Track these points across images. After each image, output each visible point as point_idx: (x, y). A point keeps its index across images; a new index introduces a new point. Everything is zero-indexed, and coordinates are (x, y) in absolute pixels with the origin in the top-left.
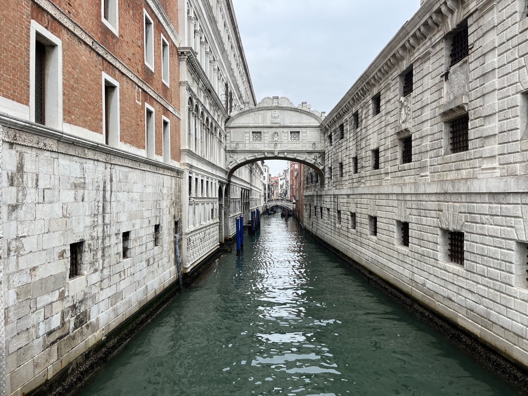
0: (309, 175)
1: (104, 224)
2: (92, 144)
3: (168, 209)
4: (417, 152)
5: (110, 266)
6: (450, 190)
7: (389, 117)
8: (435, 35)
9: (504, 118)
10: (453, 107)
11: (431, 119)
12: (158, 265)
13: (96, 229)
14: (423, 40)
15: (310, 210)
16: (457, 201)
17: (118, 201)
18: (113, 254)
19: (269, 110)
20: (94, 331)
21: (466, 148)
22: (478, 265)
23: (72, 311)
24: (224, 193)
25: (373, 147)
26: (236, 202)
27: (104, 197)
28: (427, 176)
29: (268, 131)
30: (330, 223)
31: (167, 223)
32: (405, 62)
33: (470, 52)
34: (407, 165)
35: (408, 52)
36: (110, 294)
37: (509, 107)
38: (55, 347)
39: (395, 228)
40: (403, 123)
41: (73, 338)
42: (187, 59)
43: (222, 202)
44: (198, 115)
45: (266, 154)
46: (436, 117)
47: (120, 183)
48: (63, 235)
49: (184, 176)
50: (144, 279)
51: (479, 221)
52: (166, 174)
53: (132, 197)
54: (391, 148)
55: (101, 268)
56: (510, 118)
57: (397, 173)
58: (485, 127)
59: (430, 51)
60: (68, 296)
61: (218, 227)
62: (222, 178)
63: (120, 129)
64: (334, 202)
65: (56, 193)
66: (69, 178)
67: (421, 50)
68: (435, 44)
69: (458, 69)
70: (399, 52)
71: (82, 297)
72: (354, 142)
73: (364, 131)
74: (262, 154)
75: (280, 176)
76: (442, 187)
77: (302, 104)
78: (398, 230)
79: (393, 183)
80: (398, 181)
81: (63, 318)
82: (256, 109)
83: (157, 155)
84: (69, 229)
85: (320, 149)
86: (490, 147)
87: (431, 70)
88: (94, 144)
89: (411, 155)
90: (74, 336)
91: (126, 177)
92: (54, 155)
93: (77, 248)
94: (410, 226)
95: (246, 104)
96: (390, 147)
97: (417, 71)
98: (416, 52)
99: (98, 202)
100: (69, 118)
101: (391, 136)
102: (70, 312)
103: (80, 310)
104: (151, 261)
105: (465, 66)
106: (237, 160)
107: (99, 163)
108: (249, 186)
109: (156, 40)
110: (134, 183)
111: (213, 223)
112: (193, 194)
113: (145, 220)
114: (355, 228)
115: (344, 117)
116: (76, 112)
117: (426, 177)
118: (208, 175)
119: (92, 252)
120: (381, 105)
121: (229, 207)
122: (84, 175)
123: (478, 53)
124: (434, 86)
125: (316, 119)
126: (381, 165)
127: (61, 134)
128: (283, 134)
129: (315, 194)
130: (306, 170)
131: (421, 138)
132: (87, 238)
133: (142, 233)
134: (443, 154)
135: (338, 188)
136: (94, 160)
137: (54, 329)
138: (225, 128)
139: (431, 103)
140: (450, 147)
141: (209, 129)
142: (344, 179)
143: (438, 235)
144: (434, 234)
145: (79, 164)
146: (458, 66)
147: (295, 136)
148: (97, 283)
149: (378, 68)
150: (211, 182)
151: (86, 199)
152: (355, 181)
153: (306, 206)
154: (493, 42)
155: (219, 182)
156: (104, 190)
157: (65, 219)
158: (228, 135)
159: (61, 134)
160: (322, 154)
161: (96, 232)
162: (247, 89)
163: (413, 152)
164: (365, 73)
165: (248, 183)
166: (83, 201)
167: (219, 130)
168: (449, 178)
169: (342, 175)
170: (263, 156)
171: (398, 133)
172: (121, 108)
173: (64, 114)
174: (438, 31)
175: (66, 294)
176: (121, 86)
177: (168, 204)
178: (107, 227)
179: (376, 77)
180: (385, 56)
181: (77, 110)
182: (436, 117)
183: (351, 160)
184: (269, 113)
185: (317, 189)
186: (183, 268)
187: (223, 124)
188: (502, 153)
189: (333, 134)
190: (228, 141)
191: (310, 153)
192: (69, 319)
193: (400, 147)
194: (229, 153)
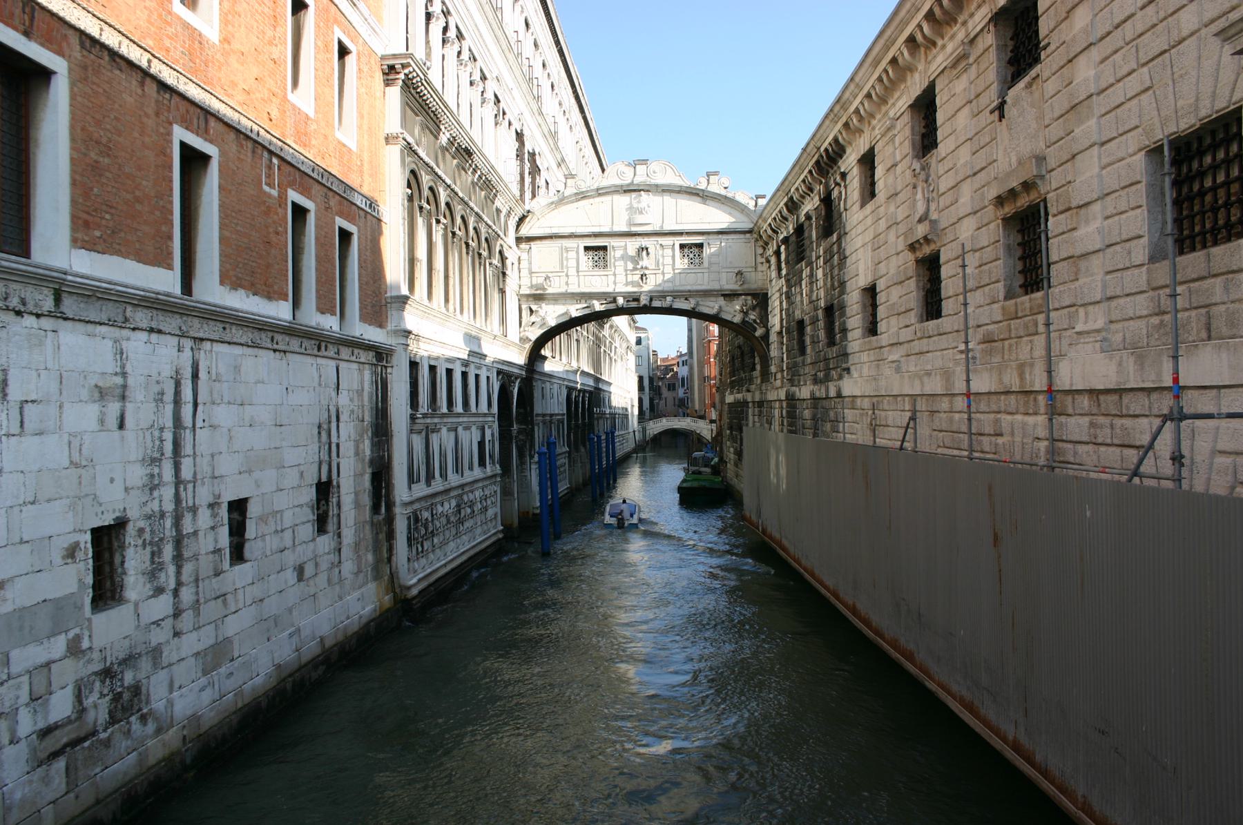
0: (738, 352)
1: (178, 481)
2: (142, 293)
3: (352, 443)
5: (197, 580)
7: (892, 209)
8: (972, 15)
9: (1115, 212)
13: (156, 494)
14: (950, 26)
17: (213, 427)
18: (203, 552)
19: (625, 191)
23: (103, 682)
25: (863, 281)
26: (551, 422)
31: (352, 478)
32: (917, 75)
34: (932, 324)
36: (200, 647)
37: (1122, 185)
38: (61, 764)
40: (920, 221)
41: (107, 743)
47: (216, 383)
48: (72, 507)
49: (394, 360)
50: (290, 610)
51: (1072, 460)
52: (346, 358)
53: (252, 417)
55: (172, 585)
60: (90, 648)
63: (220, 255)
65: (53, 410)
66: (85, 377)
67: (950, 48)
68: (976, 36)
70: (902, 54)
71: (128, 652)
76: (1000, 379)
77: (708, 176)
80: (916, 365)
81: (79, 697)
82: (592, 190)
83: (323, 313)
84: (87, 495)
86: (1088, 280)
88: (148, 294)
89: (941, 300)
90: (109, 739)
91: (235, 367)
92: (46, 323)
93: (114, 539)
97: (945, 99)
99: (162, 429)
100: (86, 238)
102: (98, 684)
103: (122, 680)
107: (162, 337)
109: (319, 43)
111: (482, 476)
112: (424, 407)
113: (288, 470)
115: (803, 207)
116: (104, 222)
119: (148, 549)
120: (876, 179)
122: (123, 367)
126: (882, 327)
127: (64, 276)
128: (661, 252)
129: (749, 397)
132: (133, 514)
133: (282, 501)
134: (1001, 297)
140: (1021, 281)
141: (467, 245)
145: (110, 343)
147: (691, 256)
148: (163, 620)
149: (865, 91)
150: (477, 376)
155: (499, 372)
156: (177, 402)
157: (73, 471)
158: (524, 256)
159: (64, 276)
161: (156, 502)
163: (943, 294)
164: (838, 101)
166: (121, 426)
169: (802, 351)
170: (612, 306)
171: (912, 247)
172: (223, 206)
175: (85, 644)
176: (223, 153)
177: (352, 431)
178: (185, 489)
179: (862, 112)
180: (876, 63)
181: (108, 216)
182: (986, 207)
184: (623, 201)
185: (753, 387)
186: (400, 586)
189: (783, 248)
190: (525, 272)
191: (730, 296)
193: (918, 281)
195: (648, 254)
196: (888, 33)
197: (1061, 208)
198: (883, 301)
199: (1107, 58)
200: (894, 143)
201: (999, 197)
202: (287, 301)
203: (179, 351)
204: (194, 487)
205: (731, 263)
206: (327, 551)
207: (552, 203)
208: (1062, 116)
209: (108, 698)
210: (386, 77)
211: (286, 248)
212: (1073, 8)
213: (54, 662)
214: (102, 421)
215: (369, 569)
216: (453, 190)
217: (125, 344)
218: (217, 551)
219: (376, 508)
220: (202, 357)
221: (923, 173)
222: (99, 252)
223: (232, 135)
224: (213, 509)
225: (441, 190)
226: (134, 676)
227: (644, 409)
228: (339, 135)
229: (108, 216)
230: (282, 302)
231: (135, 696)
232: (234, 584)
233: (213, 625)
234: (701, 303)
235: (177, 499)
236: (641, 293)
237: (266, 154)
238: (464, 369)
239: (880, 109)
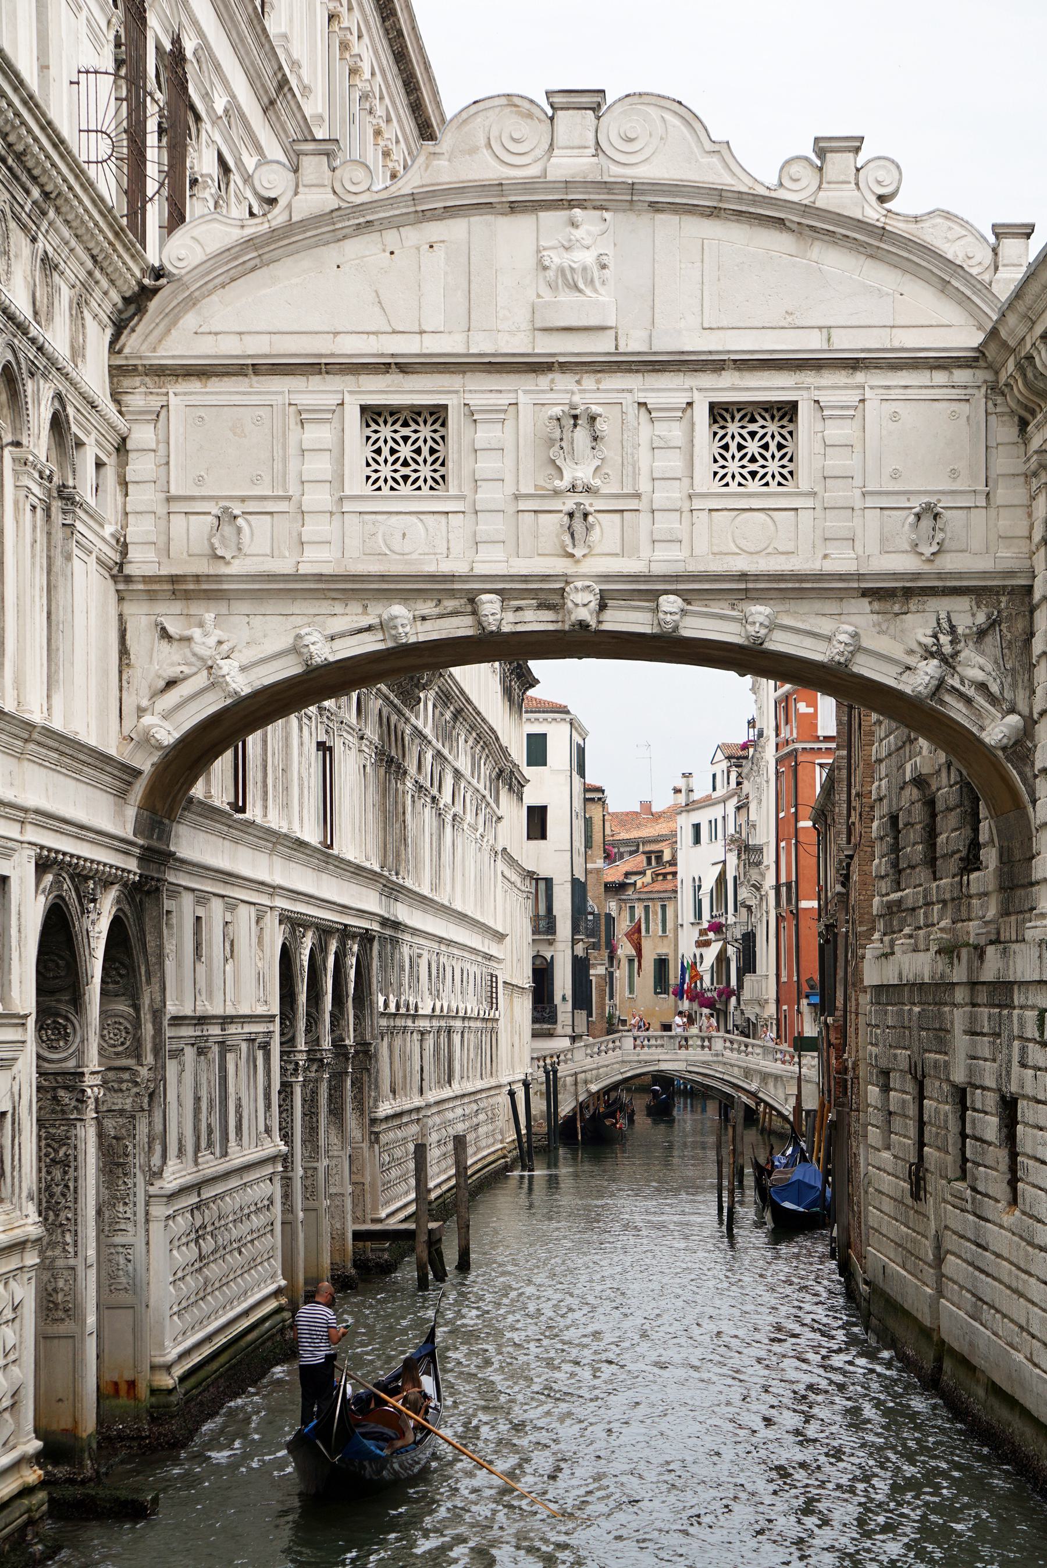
15: (921, 1124)
19: (514, 208)
24: (96, 967)
26: (224, 1047)
29: (504, 400)
43: (80, 1053)
45: (490, 604)
62: (81, 830)
74: (450, 604)
75: (690, 807)
82: (393, 201)
85: (984, 564)
95: (307, 162)
106: (228, 668)
108: (370, 900)
121: (155, 1095)
125: (944, 286)
128: (645, 431)
130: (879, 749)
138: (117, 372)
147: (753, 447)
153: (886, 1089)
158: (142, 435)
162: (350, 20)
165: (357, 872)
167: (47, 391)
170: (460, 627)
187: (98, 338)
190: (141, 497)
194: (152, 596)
195: (595, 439)
205: (895, 476)
207: (250, 243)
227: (557, 999)
234: (787, 621)
236: (567, 579)
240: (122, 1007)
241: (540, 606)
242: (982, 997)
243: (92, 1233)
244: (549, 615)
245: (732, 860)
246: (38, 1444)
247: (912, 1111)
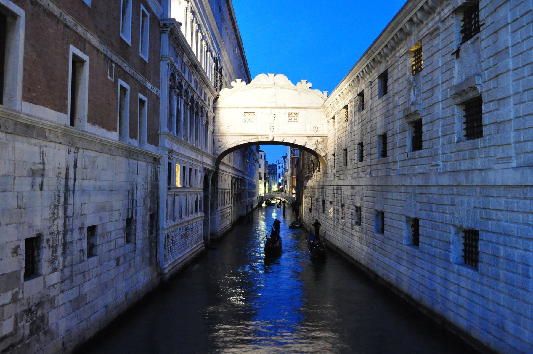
1: (66, 217)
3: (142, 200)
4: (428, 139)
5: (72, 265)
6: (464, 182)
8: (443, 10)
10: (465, 88)
11: (442, 101)
12: (130, 265)
13: (56, 222)
15: (311, 203)
16: (471, 194)
17: (83, 191)
20: (52, 339)
21: (479, 135)
22: (493, 268)
23: (28, 315)
25: (380, 132)
27: (66, 186)
28: (438, 165)
30: (333, 218)
31: (141, 217)
33: (481, 28)
34: (417, 153)
35: (416, 27)
36: (72, 298)
39: (404, 225)
40: (412, 104)
41: (28, 345)
42: (170, 31)
44: (181, 93)
46: (448, 99)
51: (494, 218)
54: (400, 133)
55: (61, 267)
56: (525, 102)
57: (406, 162)
58: (500, 112)
59: (439, 26)
60: (22, 298)
61: (202, 223)
64: (337, 194)
67: (430, 25)
68: (445, 19)
69: (470, 47)
72: (360, 126)
73: (369, 113)
74: (255, 137)
75: (279, 164)
78: (408, 227)
79: (402, 173)
80: (408, 171)
81: (16, 323)
83: (132, 138)
87: (441, 47)
89: (422, 141)
94: (421, 222)
96: (398, 132)
98: (424, 27)
99: (59, 191)
100: (29, 97)
101: (399, 119)
102: (25, 316)
103: (36, 314)
104: (121, 261)
105: (477, 43)
108: (241, 175)
110: (103, 170)
114: (360, 225)
116: (37, 89)
117: (438, 167)
118: (191, 161)
119: (51, 249)
120: (388, 85)
122: (43, 160)
123: (491, 30)
124: (444, 64)
126: (389, 153)
130: (306, 157)
131: (432, 122)
133: (111, 227)
134: (456, 141)
135: (342, 178)
136: (57, 143)
137: (6, 335)
139: (442, 83)
140: (464, 132)
141: (194, 109)
142: (349, 167)
143: (450, 233)
144: (447, 232)
145: (37, 149)
146: (470, 44)
147: (293, 118)
148: (56, 284)
150: (196, 170)
151: (45, 187)
152: (360, 170)
154: (506, 18)
156: (67, 178)
159: (19, 114)
160: (325, 138)
161: (55, 226)
163: (423, 138)
166: (41, 189)
168: (463, 168)
169: (346, 164)
171: (407, 117)
172: (90, 84)
173: (23, 92)
174: (447, 5)
175: (20, 296)
176: (91, 60)
177: (143, 194)
178: (69, 220)
179: (382, 54)
181: (39, 87)
182: (448, 99)
183: (356, 146)
188: (518, 141)
189: (336, 117)
192: (23, 325)
196: (399, 17)
197: (490, 100)
198: (390, 141)
199: (516, 31)
200: (398, 68)
201: (456, 94)
202: (116, 131)
203: (69, 153)
204: (73, 219)
206: (130, 251)
208: (491, 57)
209: (28, 324)
210: (161, 29)
211: (117, 106)
212: (498, 7)
213: (6, 305)
214: (33, 186)
215: (147, 260)
216: (188, 84)
217: (45, 149)
218: (82, 251)
219: (151, 232)
220: (79, 156)
221: (414, 82)
222: (34, 104)
223: (95, 52)
224: (81, 230)
225: (184, 84)
226: (42, 312)
228: (141, 55)
229: (39, 87)
230: (114, 132)
231: (42, 322)
232: (88, 267)
233: (78, 287)
235: (65, 225)
237: (109, 61)
238: (190, 167)
239: (391, 53)
240: (213, 187)
241: (266, 138)
242: (320, 187)
243: (209, 215)
244: (267, 139)
245: (284, 171)
246: (203, 241)
247: (310, 202)
